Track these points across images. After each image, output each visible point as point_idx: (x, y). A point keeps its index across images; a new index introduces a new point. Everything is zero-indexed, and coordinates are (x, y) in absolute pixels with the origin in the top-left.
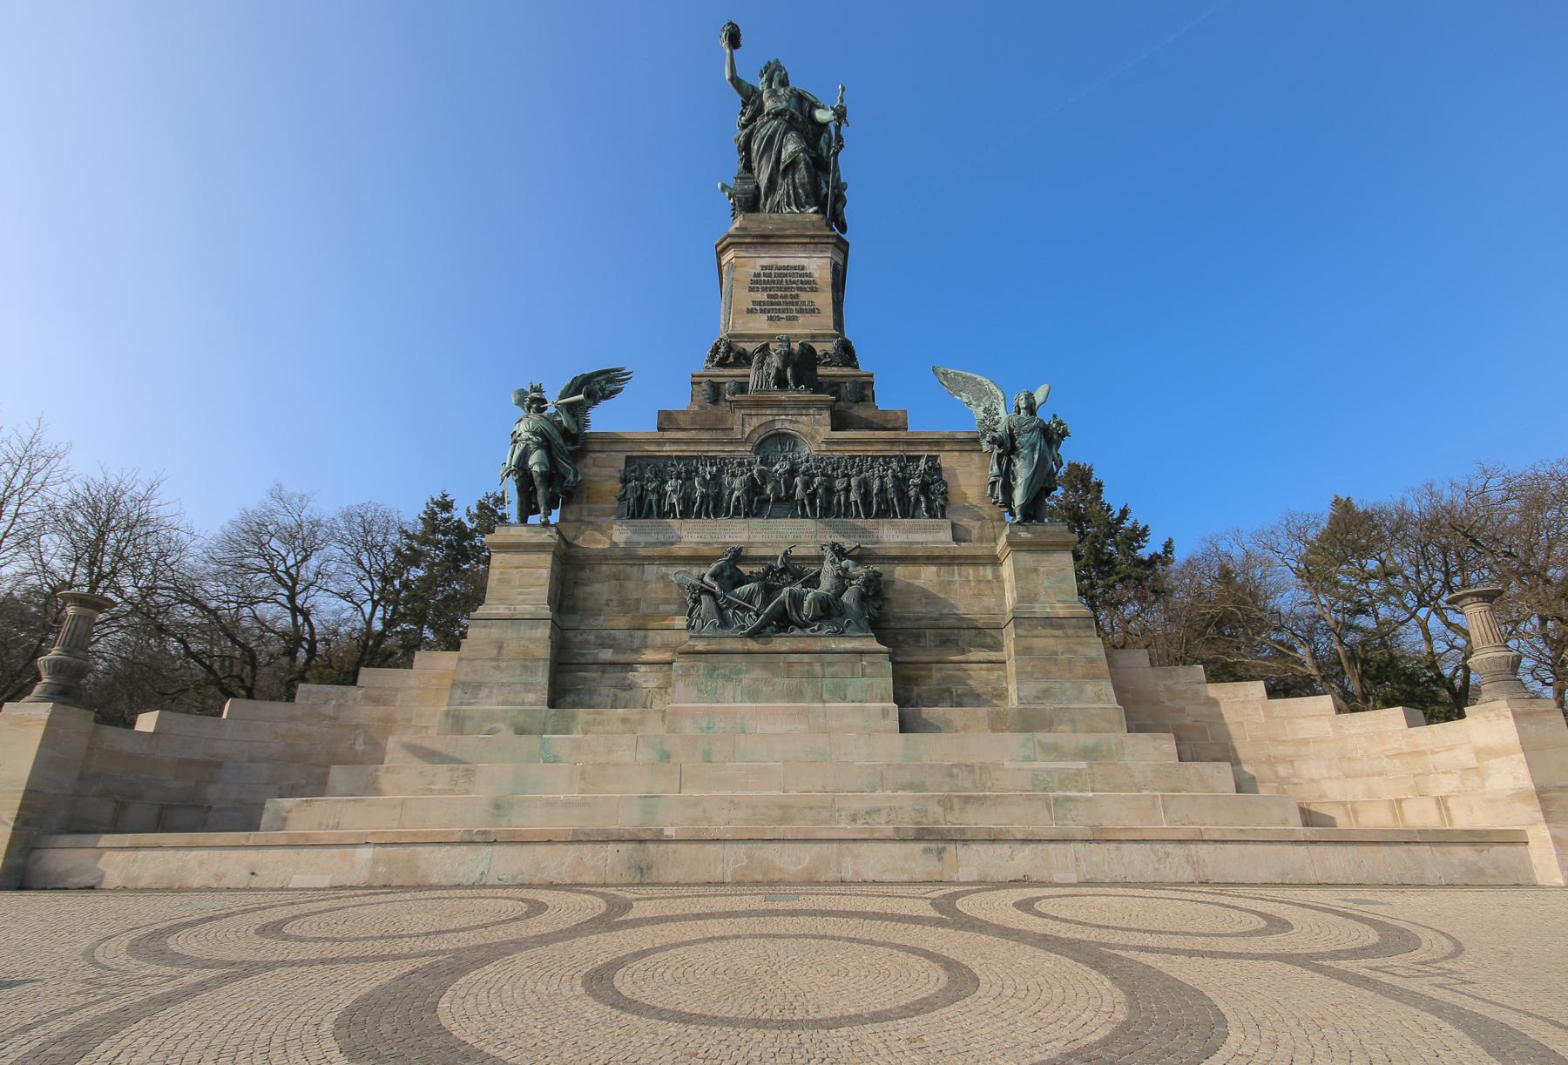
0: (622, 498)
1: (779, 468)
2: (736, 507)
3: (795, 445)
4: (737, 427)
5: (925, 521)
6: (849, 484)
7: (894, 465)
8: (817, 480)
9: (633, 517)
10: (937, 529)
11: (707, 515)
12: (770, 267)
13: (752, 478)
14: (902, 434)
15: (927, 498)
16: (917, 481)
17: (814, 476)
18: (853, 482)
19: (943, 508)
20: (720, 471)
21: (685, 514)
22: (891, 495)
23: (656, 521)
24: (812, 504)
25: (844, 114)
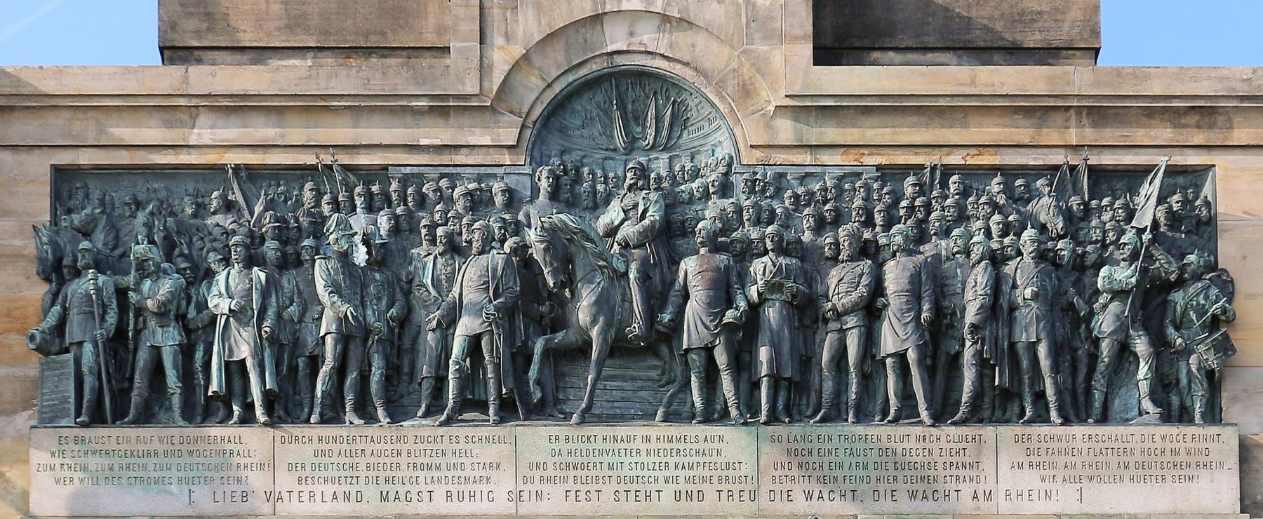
0: (53, 343)
1: (622, 217)
2: (470, 379)
3: (680, 120)
4: (463, 45)
5: (1144, 434)
6: (877, 288)
7: (1044, 208)
8: (760, 268)
9: (98, 418)
10: (1182, 468)
11: (365, 411)
13: (523, 261)
14: (1076, 79)
15: (1160, 343)
18: (895, 276)
19: (1213, 380)
21: (284, 408)
22: (1029, 327)
23: (180, 432)
24: (742, 363)
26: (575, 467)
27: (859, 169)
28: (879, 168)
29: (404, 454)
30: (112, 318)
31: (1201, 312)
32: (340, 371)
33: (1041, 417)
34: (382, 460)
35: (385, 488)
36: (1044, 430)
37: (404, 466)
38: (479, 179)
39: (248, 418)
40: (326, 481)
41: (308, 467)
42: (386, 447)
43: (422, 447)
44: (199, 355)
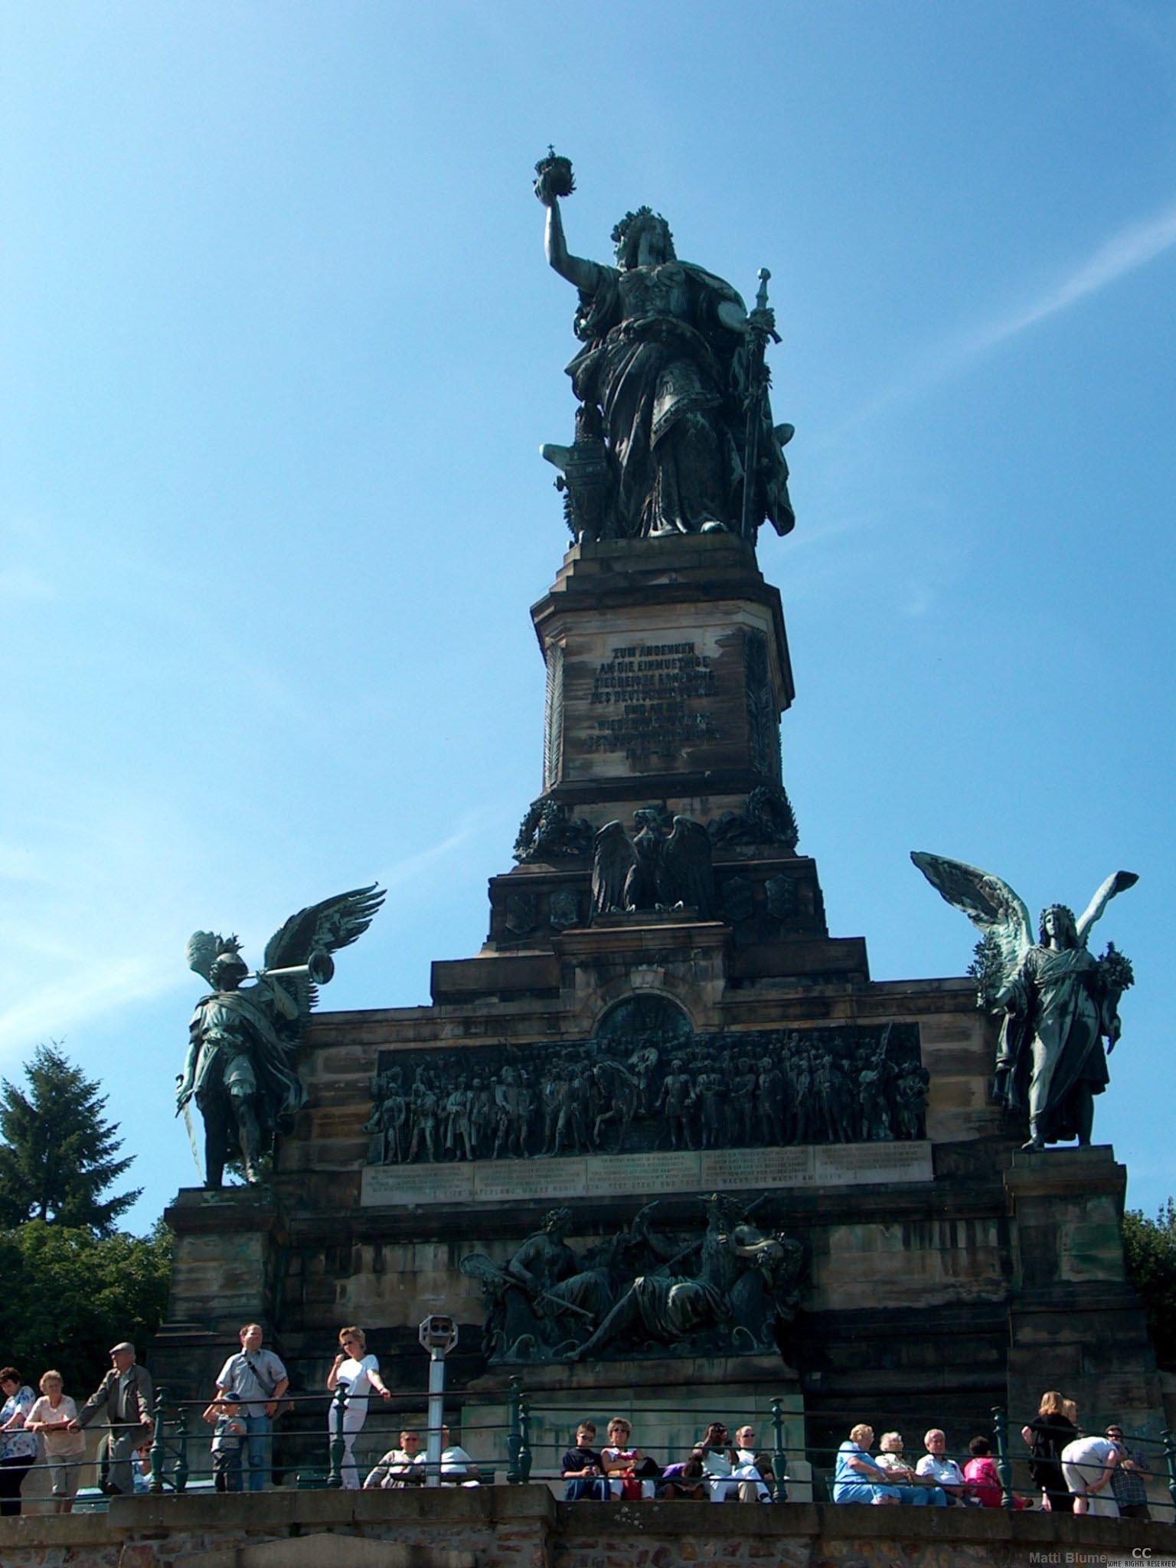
6: (757, 1086)
9: (395, 1162)
10: (904, 1161)
12: (631, 651)
16: (868, 1076)
17: (694, 1074)
20: (539, 1073)
21: (482, 1152)
24: (694, 1120)
25: (771, 322)
30: (403, 1117)
31: (911, 1088)
32: (507, 1134)
33: (837, 1140)
36: (838, 1146)
38: (573, 1046)
39: (463, 1158)
44: (442, 1129)
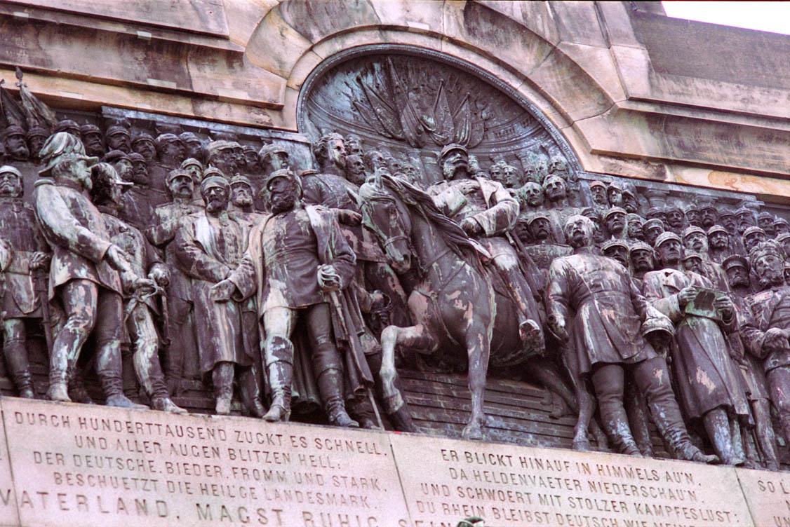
26: (491, 494)
27: (737, 196)
28: (759, 196)
29: (224, 453)
34: (190, 460)
35: (204, 499)
37: (227, 471)
40: (102, 481)
41: (69, 460)
42: (193, 442)
43: (252, 448)
